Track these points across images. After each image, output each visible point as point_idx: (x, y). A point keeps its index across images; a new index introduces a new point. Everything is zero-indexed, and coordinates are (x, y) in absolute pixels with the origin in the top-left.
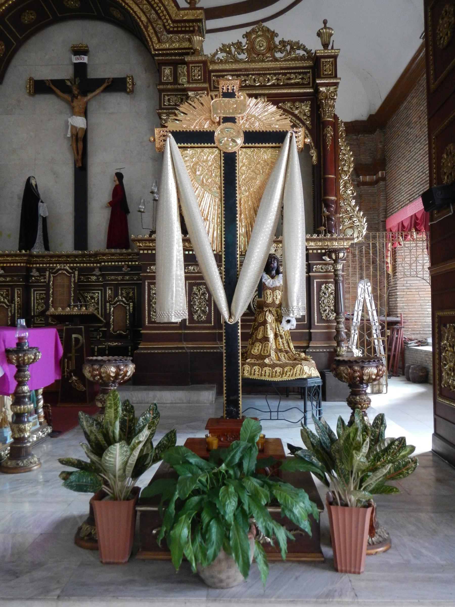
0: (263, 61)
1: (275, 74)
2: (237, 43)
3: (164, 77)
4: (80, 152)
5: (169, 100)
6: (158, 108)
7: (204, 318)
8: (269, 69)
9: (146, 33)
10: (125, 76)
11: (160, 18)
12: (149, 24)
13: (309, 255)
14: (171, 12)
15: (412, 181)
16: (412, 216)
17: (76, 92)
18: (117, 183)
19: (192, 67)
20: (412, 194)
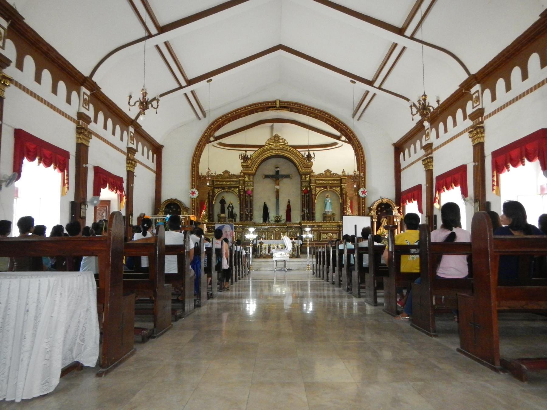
1: (331, 181)
5: (304, 184)
7: (316, 239)
8: (329, 179)
10: (289, 174)
11: (302, 163)
18: (288, 204)
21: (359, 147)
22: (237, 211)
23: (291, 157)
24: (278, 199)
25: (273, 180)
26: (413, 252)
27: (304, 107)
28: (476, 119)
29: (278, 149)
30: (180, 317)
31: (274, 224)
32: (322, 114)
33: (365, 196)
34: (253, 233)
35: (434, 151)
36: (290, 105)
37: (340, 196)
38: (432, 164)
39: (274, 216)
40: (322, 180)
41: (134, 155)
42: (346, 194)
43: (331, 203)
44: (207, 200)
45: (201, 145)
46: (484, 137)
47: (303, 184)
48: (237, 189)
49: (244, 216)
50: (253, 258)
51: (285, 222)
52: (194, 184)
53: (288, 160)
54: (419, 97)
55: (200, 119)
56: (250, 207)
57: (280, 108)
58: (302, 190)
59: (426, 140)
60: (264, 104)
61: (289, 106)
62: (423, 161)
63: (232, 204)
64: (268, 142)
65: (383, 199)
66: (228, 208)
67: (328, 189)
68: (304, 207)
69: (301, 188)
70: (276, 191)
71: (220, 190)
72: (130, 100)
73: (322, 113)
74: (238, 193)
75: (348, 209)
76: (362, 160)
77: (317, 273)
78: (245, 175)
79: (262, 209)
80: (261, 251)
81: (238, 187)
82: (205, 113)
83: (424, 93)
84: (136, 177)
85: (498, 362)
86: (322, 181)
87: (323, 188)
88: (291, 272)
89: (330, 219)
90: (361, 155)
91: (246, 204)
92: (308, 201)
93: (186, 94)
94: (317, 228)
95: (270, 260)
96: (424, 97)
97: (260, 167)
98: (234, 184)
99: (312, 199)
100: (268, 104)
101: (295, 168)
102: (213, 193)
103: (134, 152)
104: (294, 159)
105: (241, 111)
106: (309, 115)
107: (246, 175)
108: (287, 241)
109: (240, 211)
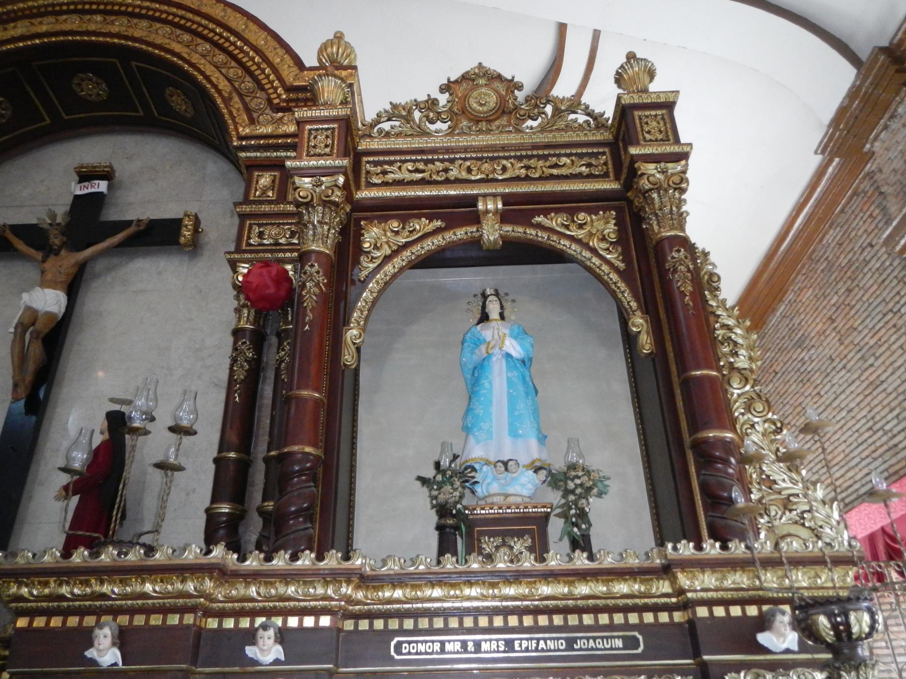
1: (520, 158)
2: (427, 101)
3: (256, 190)
4: (31, 367)
6: (233, 249)
8: (504, 148)
9: (225, 111)
11: (261, 88)
12: (234, 94)
13: (699, 627)
14: (284, 74)
15: (842, 456)
16: (872, 538)
17: (57, 241)
19: (310, 130)
20: (851, 486)
37: (627, 297)
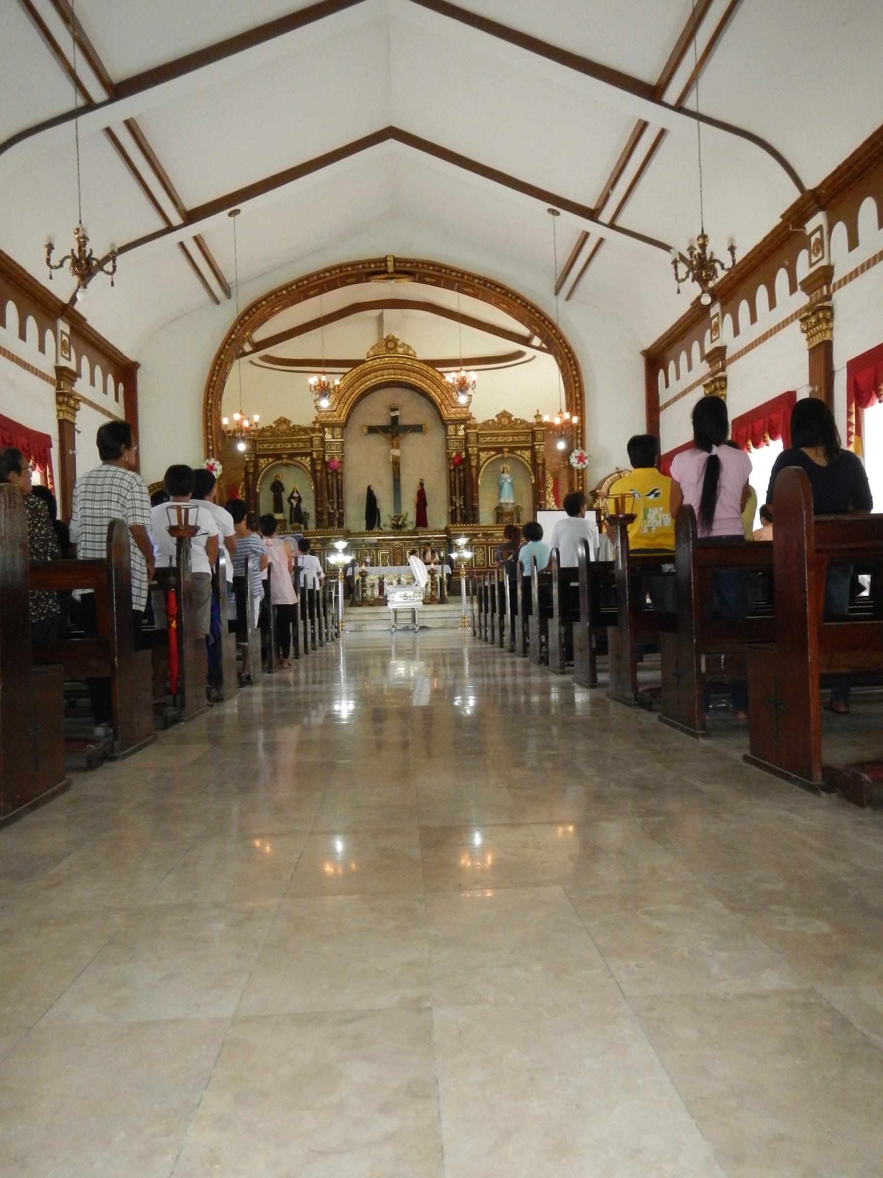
0: (506, 429)
1: (512, 436)
5: (453, 445)
7: (482, 564)
11: (448, 399)
18: (420, 488)
21: (569, 360)
22: (308, 506)
23: (423, 385)
24: (399, 479)
25: (385, 437)
26: (666, 571)
27: (448, 271)
28: (818, 288)
29: (394, 369)
30: (176, 721)
31: (390, 534)
32: (490, 287)
33: (584, 466)
34: (346, 551)
35: (730, 364)
36: (417, 266)
38: (724, 393)
39: (389, 516)
40: (493, 435)
41: (73, 386)
42: (543, 464)
43: (511, 484)
44: (243, 483)
45: (222, 360)
46: (831, 329)
47: (451, 443)
48: (308, 459)
49: (325, 517)
50: (345, 606)
51: (415, 528)
52: (211, 447)
53: (418, 392)
54: (691, 240)
55: (217, 302)
56: (338, 498)
57: (395, 275)
58: (449, 458)
59: (712, 341)
60: (360, 267)
61: (416, 270)
62: (706, 386)
63: (297, 492)
64: (372, 353)
65: (621, 472)
66: (289, 501)
67: (506, 455)
68: (455, 494)
69: (448, 453)
70: (393, 461)
71: (270, 460)
72: (49, 253)
73: (488, 285)
74: (309, 468)
75: (549, 498)
76: (576, 388)
77: (479, 632)
78: (324, 428)
79: (365, 500)
80: (364, 591)
81: (310, 454)
82: (230, 289)
83: (703, 231)
84: (80, 434)
85: (818, 775)
86: (493, 437)
87: (494, 453)
88: (430, 633)
89: (510, 519)
90: (574, 376)
91: (328, 488)
92: (462, 480)
93: (182, 245)
94: (483, 540)
95: (382, 609)
96: (701, 241)
97: (357, 409)
98: (302, 448)
99: (472, 477)
100: (370, 267)
101: (433, 409)
102: (254, 468)
103: (72, 377)
104: (430, 390)
105: (309, 283)
106: (460, 290)
107: (327, 427)
108: (418, 567)
109: (317, 506)
